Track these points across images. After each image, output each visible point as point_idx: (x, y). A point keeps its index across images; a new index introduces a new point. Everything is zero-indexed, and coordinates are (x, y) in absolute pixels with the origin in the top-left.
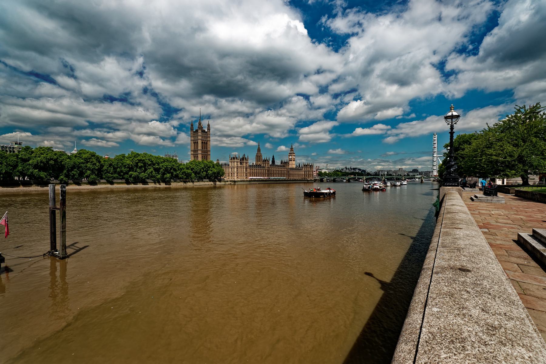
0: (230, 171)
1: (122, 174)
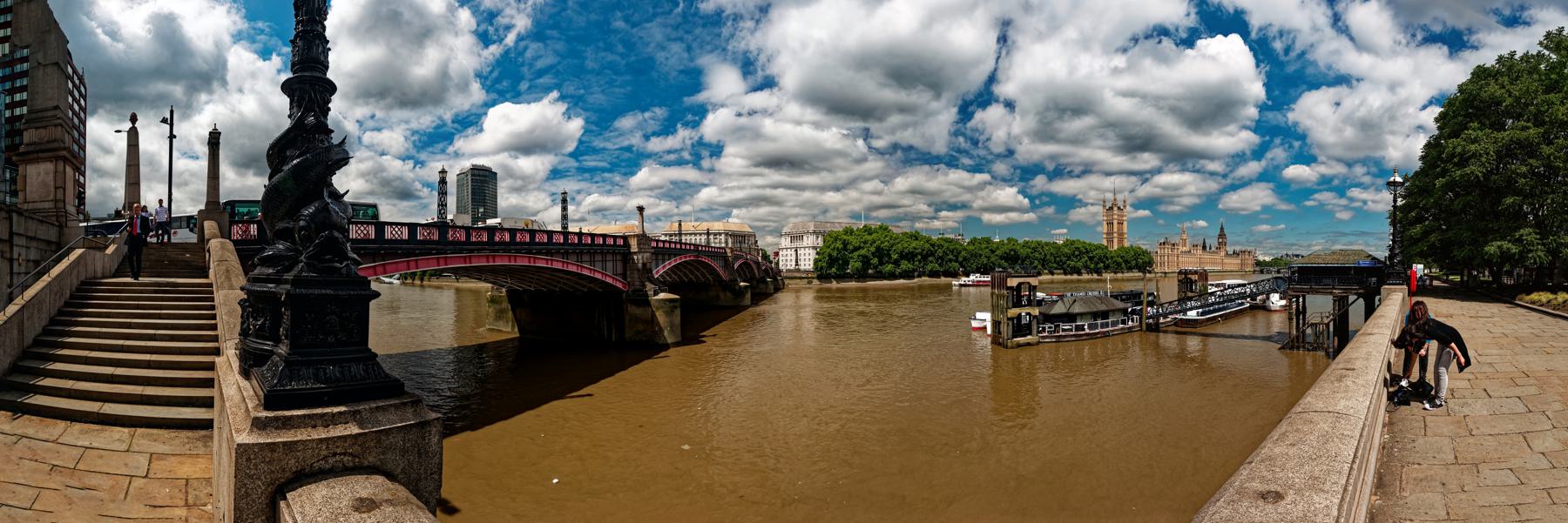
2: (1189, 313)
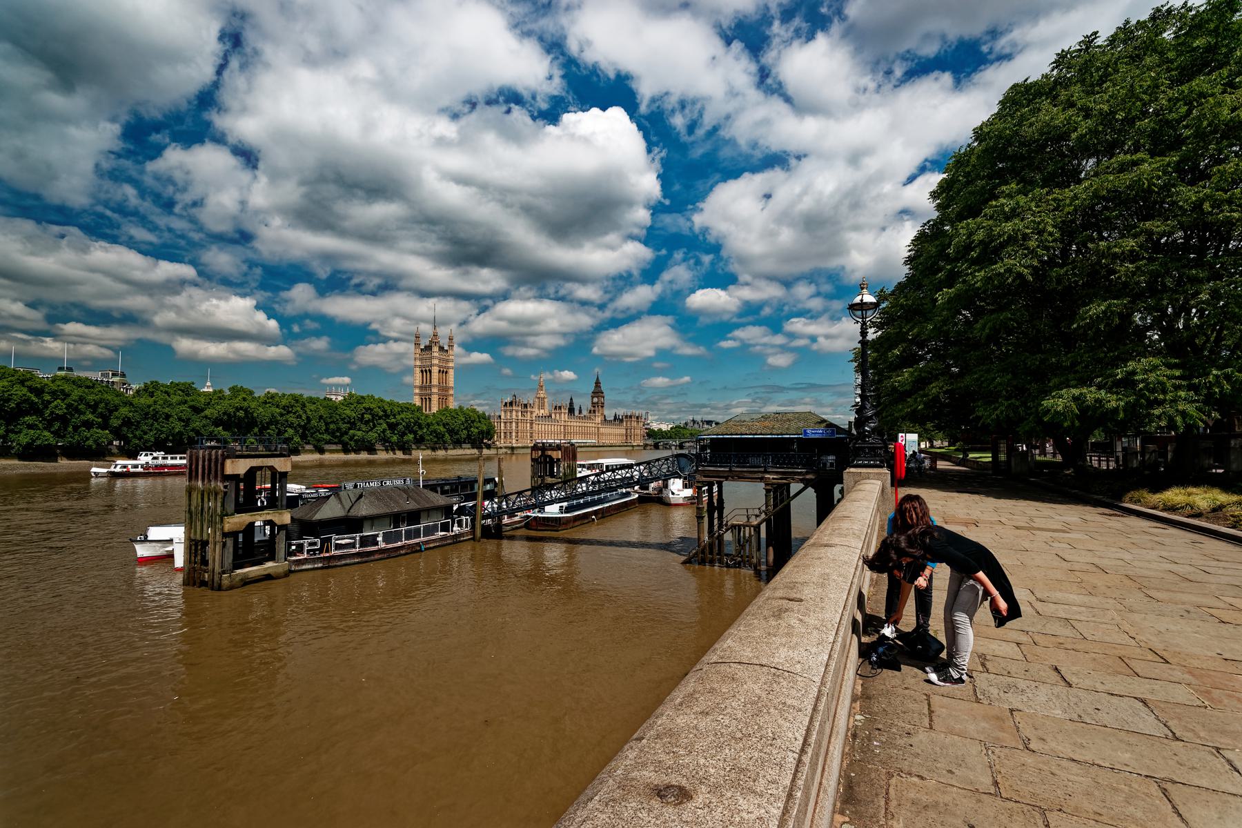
0: (502, 428)
2: (548, 508)
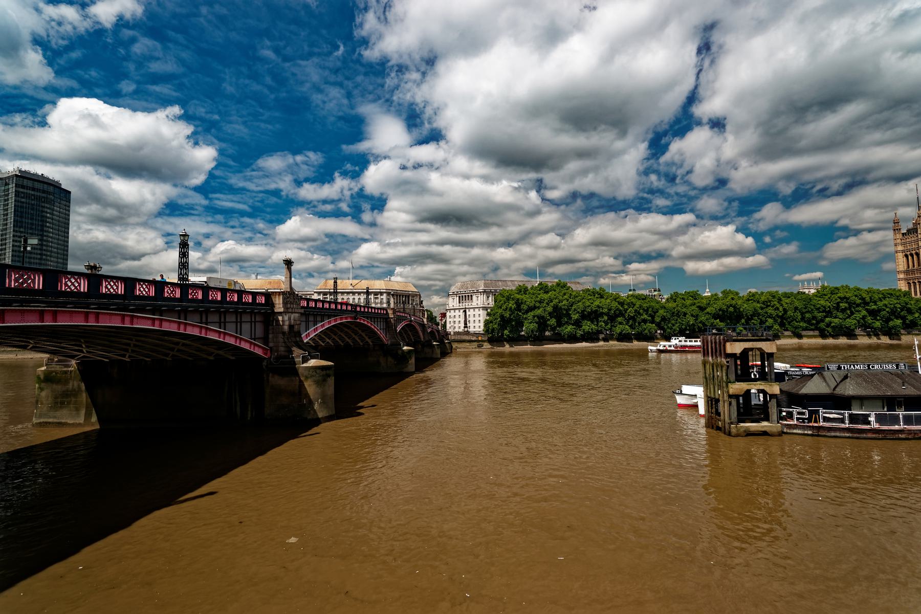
1: (814, 322)
